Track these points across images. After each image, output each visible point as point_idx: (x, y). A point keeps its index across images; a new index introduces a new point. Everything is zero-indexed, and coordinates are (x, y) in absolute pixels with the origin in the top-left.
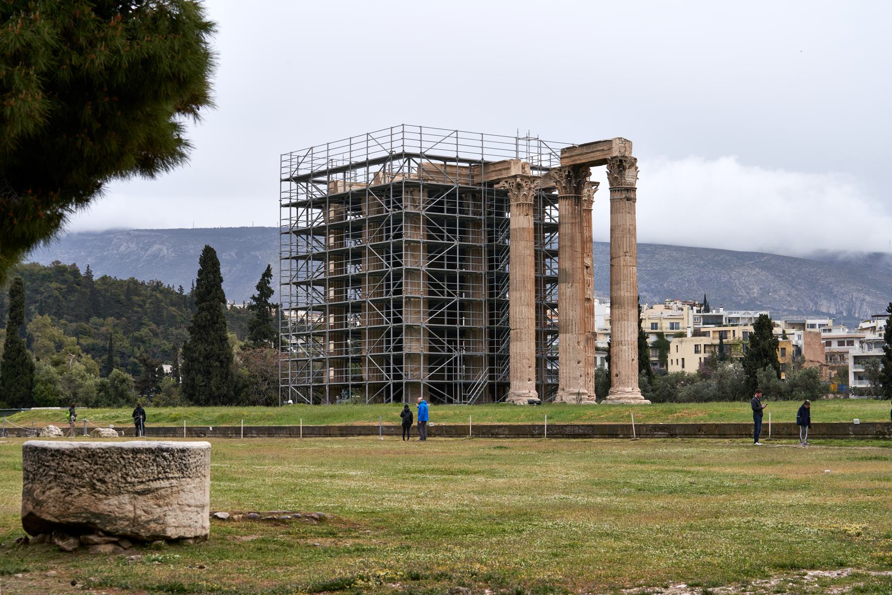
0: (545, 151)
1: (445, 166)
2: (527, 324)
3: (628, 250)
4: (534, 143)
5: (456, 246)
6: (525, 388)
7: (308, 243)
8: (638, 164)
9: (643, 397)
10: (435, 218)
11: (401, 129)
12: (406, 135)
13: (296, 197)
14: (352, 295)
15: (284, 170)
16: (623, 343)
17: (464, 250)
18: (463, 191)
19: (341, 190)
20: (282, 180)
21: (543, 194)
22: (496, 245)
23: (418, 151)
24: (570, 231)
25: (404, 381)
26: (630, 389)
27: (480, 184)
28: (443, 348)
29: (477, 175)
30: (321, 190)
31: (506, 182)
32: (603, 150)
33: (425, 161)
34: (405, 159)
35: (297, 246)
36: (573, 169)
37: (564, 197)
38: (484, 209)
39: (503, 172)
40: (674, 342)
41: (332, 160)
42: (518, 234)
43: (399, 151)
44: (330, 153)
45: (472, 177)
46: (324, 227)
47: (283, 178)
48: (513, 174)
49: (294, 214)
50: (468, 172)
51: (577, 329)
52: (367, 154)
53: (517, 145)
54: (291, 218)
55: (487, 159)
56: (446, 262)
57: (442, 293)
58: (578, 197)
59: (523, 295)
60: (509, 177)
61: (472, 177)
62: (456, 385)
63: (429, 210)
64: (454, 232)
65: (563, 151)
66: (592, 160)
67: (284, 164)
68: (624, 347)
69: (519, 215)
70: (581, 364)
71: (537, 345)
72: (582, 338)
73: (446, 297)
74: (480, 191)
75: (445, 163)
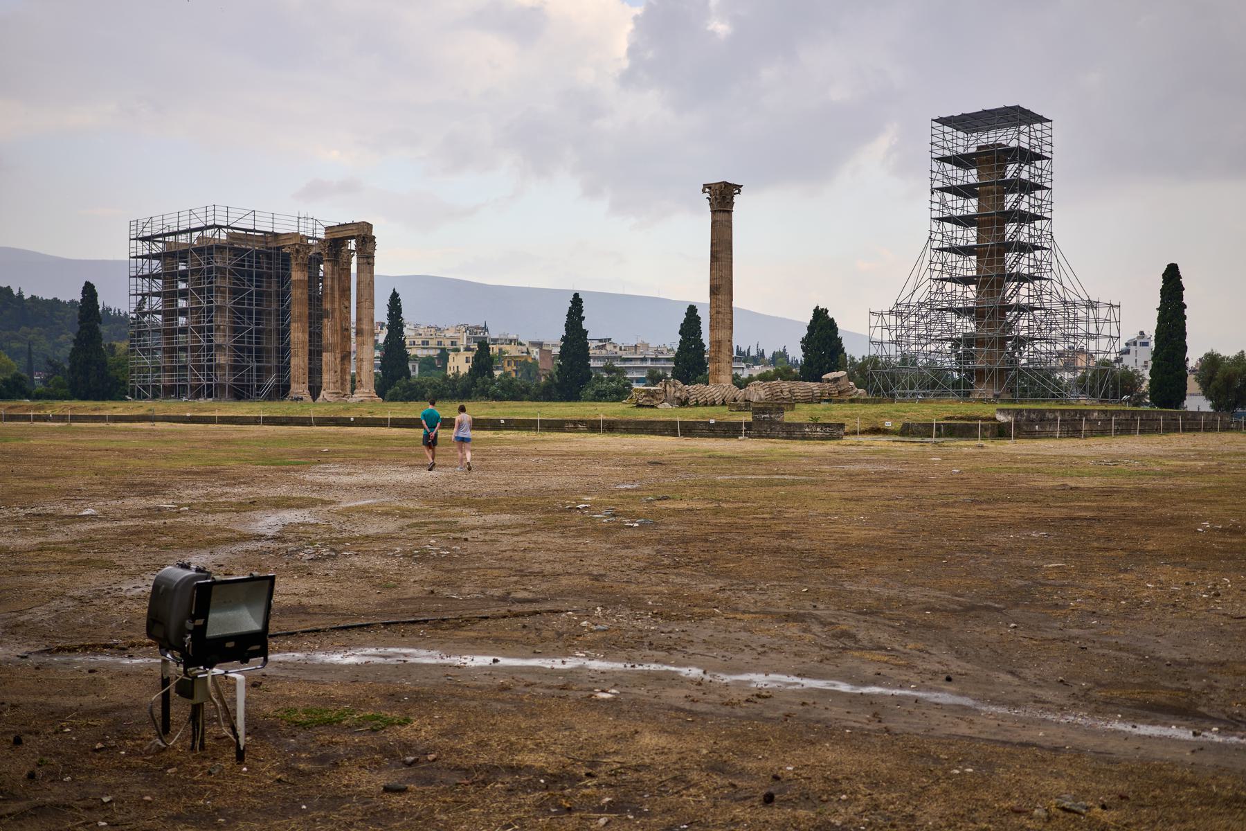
4: (310, 221)
8: (376, 240)
14: (182, 321)
19: (173, 250)
20: (130, 239)
21: (318, 256)
27: (271, 248)
28: (244, 361)
30: (158, 248)
33: (230, 231)
40: (452, 355)
45: (267, 243)
46: (160, 274)
49: (140, 264)
55: (275, 231)
57: (244, 323)
61: (267, 243)
65: (327, 228)
71: (310, 359)
74: (271, 253)
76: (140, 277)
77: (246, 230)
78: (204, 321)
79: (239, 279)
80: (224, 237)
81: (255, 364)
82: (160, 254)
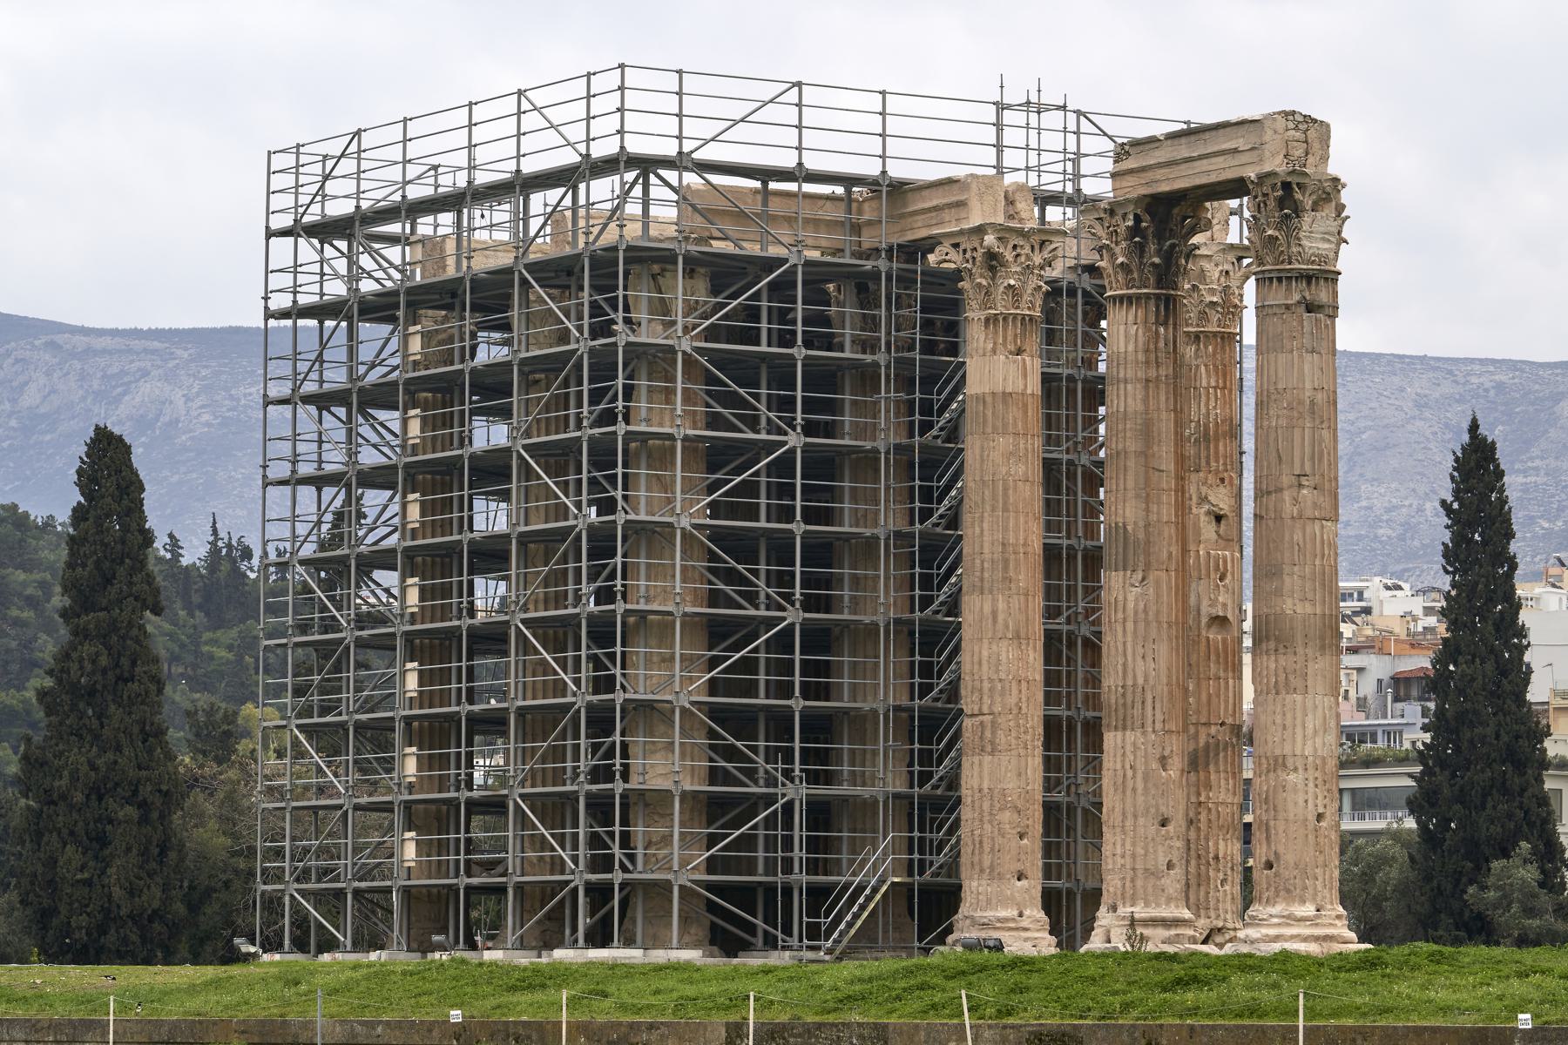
0: (1091, 144)
1: (765, 191)
2: (1012, 700)
3: (1308, 470)
5: (792, 451)
6: (1005, 902)
7: (350, 431)
8: (1345, 196)
9: (1353, 935)
10: (719, 359)
11: (614, 79)
12: (632, 100)
13: (316, 288)
15: (278, 201)
16: (1290, 763)
17: (822, 465)
18: (817, 275)
19: (451, 272)
20: (270, 234)
21: (1086, 282)
22: (922, 447)
23: (669, 149)
24: (1140, 407)
25: (617, 877)
26: (1308, 910)
28: (751, 774)
29: (870, 223)
31: (956, 246)
32: (1235, 151)
33: (691, 178)
34: (630, 176)
35: (320, 442)
36: (1148, 210)
37: (1121, 298)
38: (888, 333)
39: (946, 215)
41: (435, 168)
42: (989, 413)
43: (603, 149)
44: (414, 150)
45: (856, 229)
47: (274, 226)
48: (975, 220)
49: (309, 345)
50: (836, 213)
51: (1159, 717)
52: (519, 156)
53: (999, 126)
54: (296, 353)
55: (897, 171)
56: (763, 501)
57: (752, 598)
58: (1168, 298)
59: (1001, 605)
60: (961, 232)
61: (856, 229)
62: (788, 891)
63: (712, 334)
64: (787, 404)
65: (1124, 151)
66: (1204, 180)
67: (278, 182)
68: (1292, 777)
69: (994, 351)
70: (1170, 828)
71: (1049, 764)
72: (1176, 746)
73: (763, 612)
74: (875, 275)
75: (765, 183)
76: (308, 399)
77: (765, 174)
78: (578, 598)
79: (731, 400)
80: (665, 212)
81: (797, 792)
82: (394, 293)
